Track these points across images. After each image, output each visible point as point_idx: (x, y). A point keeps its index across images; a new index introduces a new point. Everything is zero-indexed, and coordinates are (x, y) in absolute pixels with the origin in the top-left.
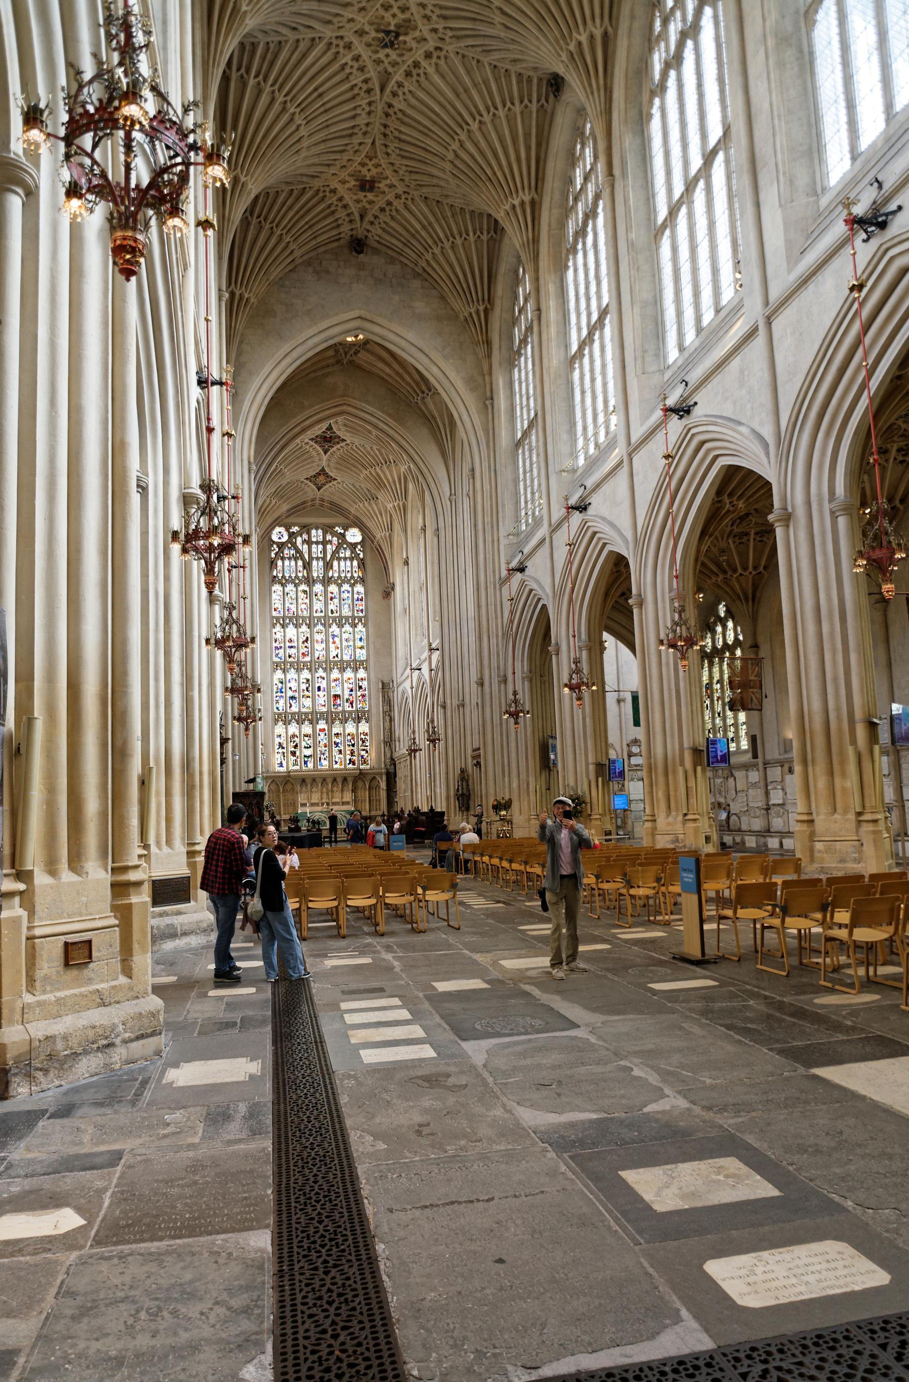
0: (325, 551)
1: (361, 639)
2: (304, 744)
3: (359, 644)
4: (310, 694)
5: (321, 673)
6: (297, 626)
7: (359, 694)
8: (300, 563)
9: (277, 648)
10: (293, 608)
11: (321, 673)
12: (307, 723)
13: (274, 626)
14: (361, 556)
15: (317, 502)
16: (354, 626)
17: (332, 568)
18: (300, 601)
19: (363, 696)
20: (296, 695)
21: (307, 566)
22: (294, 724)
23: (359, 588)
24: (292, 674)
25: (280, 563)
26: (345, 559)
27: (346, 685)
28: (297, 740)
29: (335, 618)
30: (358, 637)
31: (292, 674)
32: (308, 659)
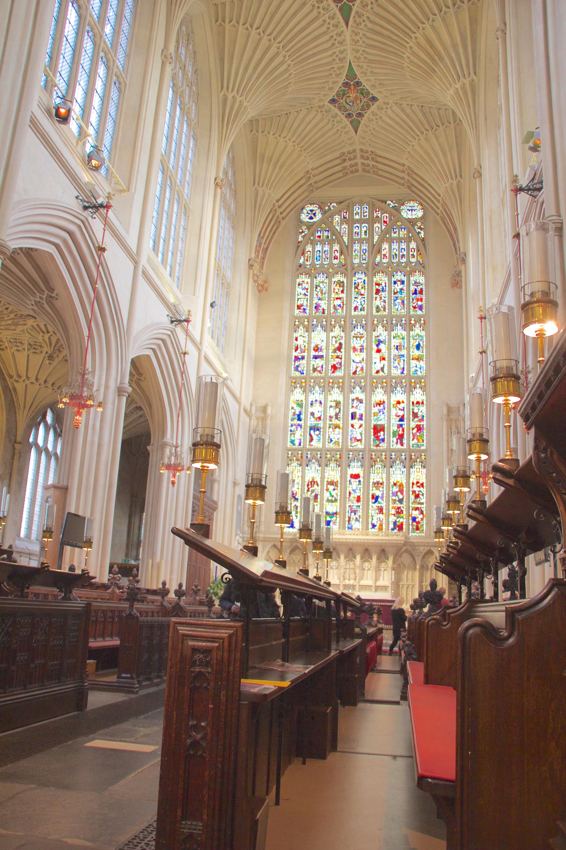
0: (371, 231)
1: (418, 347)
2: (327, 495)
3: (417, 353)
4: (340, 423)
5: (358, 393)
6: (328, 328)
7: (413, 425)
8: (336, 247)
9: (297, 358)
10: (323, 305)
11: (358, 393)
12: (333, 464)
13: (295, 328)
14: (422, 235)
15: (359, 161)
16: (409, 327)
17: (379, 251)
18: (333, 295)
19: (419, 428)
20: (321, 424)
21: (346, 250)
22: (314, 466)
23: (419, 278)
24: (317, 395)
25: (309, 248)
26: (399, 240)
27: (394, 411)
28: (317, 489)
29: (383, 317)
30: (414, 343)
31: (317, 395)
32: (338, 373)
